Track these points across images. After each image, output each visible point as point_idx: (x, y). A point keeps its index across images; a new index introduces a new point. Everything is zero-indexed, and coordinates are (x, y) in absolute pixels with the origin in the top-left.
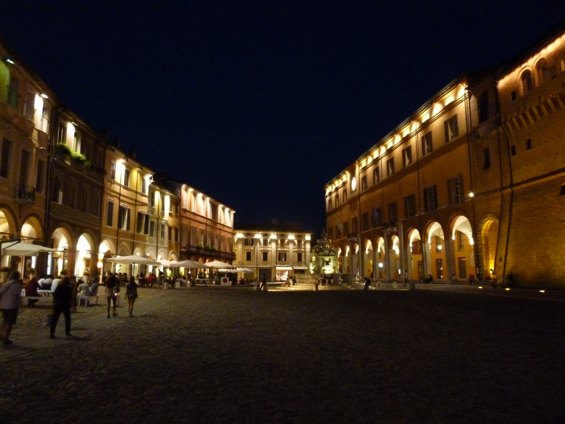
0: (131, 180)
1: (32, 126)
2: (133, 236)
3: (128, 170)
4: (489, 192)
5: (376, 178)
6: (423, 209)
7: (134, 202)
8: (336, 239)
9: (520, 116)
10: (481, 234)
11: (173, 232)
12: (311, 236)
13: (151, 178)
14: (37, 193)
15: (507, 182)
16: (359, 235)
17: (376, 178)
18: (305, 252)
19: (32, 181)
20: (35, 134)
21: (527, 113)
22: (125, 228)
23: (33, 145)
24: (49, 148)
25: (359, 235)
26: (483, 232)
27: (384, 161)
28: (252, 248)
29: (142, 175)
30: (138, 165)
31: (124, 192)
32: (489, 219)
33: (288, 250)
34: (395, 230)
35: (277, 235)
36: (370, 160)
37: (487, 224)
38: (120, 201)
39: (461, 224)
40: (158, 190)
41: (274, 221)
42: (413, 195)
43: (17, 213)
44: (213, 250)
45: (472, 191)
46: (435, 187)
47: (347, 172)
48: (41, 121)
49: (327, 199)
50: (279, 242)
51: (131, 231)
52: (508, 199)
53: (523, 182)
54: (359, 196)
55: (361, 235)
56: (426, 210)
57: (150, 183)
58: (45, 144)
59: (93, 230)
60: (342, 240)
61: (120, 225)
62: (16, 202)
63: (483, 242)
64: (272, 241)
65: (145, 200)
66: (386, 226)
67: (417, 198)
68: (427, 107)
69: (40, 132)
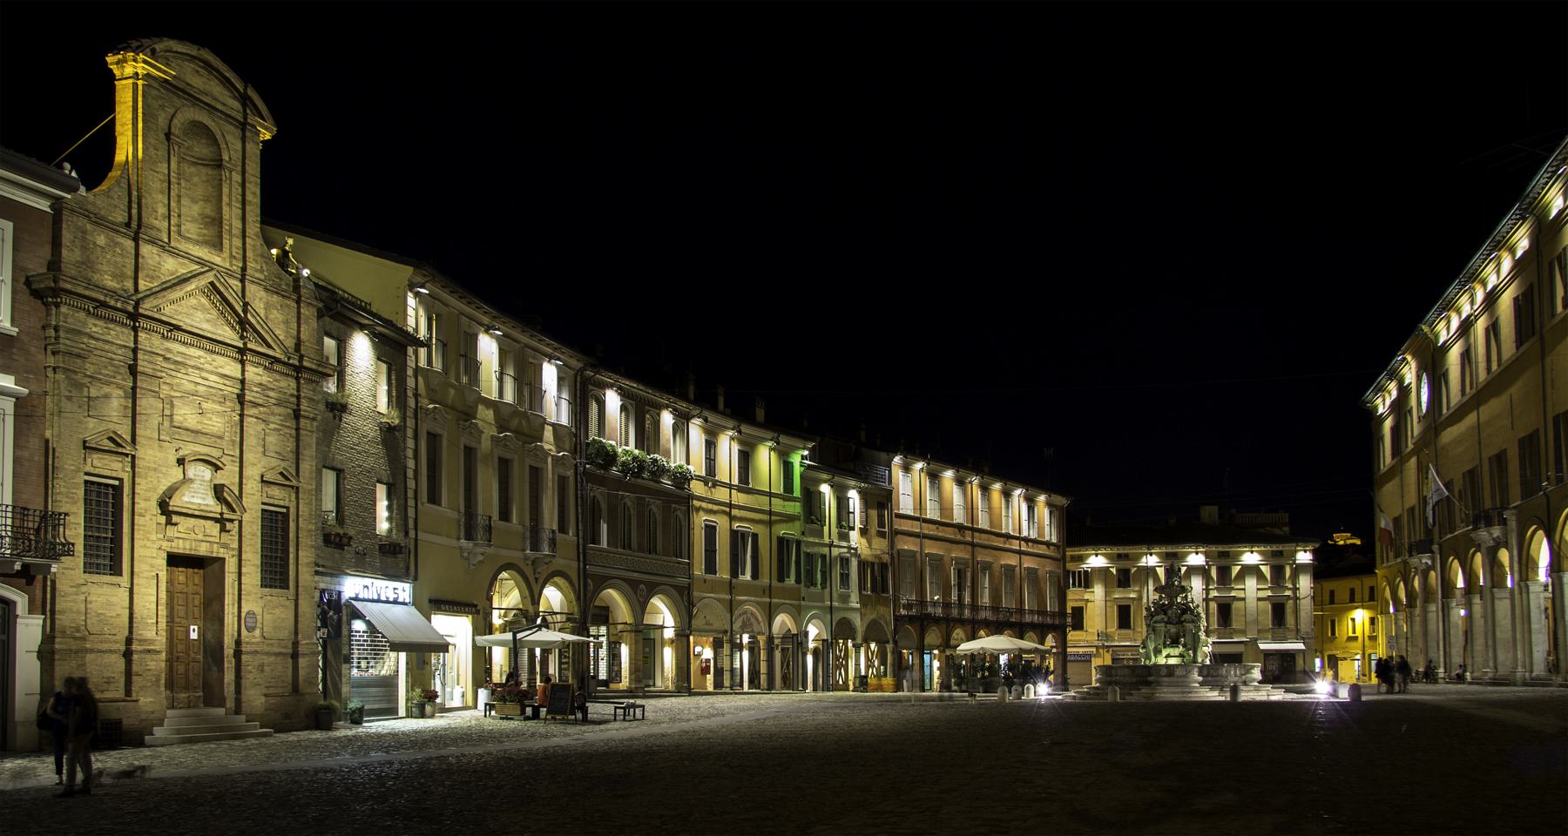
0: (755, 470)
1: (544, 422)
2: (769, 591)
7: (766, 517)
12: (1314, 552)
13: (803, 457)
14: (559, 536)
16: (1435, 547)
18: (1296, 598)
19: (550, 519)
20: (548, 433)
22: (748, 577)
23: (546, 454)
24: (574, 452)
25: (1435, 547)
28: (1133, 595)
30: (770, 435)
31: (739, 498)
33: (1241, 594)
35: (1207, 555)
41: (1210, 513)
43: (529, 572)
48: (556, 406)
55: (1440, 546)
58: (567, 446)
59: (675, 587)
61: (736, 569)
62: (526, 558)
64: (1193, 570)
69: (556, 427)
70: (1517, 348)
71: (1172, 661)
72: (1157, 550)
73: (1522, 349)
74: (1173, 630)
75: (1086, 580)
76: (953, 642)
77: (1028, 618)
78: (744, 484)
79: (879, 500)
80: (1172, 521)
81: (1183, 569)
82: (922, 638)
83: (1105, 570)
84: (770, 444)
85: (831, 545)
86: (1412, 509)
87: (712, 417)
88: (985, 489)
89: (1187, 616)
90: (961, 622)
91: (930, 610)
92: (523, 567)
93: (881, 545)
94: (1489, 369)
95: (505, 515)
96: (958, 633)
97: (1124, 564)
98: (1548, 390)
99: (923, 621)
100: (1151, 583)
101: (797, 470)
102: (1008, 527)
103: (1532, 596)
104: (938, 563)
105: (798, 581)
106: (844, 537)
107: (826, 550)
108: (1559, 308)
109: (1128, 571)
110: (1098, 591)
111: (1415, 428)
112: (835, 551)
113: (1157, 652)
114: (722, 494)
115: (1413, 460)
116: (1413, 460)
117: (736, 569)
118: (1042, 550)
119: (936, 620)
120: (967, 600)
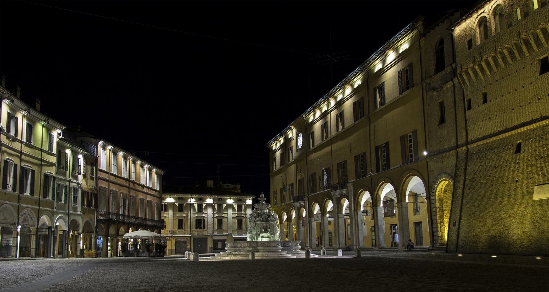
0: (35, 135)
3: (31, 123)
4: (445, 151)
5: (325, 134)
6: (374, 168)
7: (39, 162)
8: (282, 202)
9: (476, 67)
10: (435, 196)
12: (253, 200)
15: (462, 140)
16: (306, 199)
17: (325, 134)
18: (246, 218)
21: (483, 64)
25: (306, 199)
26: (437, 194)
27: (333, 114)
28: (184, 215)
29: (49, 130)
30: (44, 118)
31: (26, 150)
32: (444, 180)
33: (226, 216)
34: (344, 191)
35: (213, 199)
36: (318, 114)
37: (443, 184)
39: (415, 184)
40: (68, 148)
41: (210, 183)
42: (365, 153)
44: (137, 218)
45: (426, 150)
46: (387, 144)
47: (293, 127)
50: (216, 207)
51: (36, 196)
52: (462, 156)
53: (479, 140)
56: (378, 170)
57: (58, 139)
60: (287, 205)
63: (438, 205)
64: (208, 205)
65: (53, 159)
66: (335, 188)
67: (368, 156)
68: (380, 55)
70: (355, 121)
71: (265, 239)
72: (195, 196)
73: (357, 122)
74: (265, 225)
75: (165, 208)
76: (120, 233)
77: (149, 223)
78: (29, 143)
79: (92, 161)
80: (197, 186)
81: (204, 205)
83: (173, 204)
84: (43, 123)
85: (70, 181)
86: (292, 185)
87: (16, 101)
88: (134, 163)
89: (271, 218)
90: (124, 223)
91: (111, 217)
93: (92, 183)
94: (337, 130)
96: (122, 229)
97: (181, 202)
98: (372, 137)
99: (108, 222)
100: (192, 210)
101: (55, 140)
102: (142, 182)
103: (359, 216)
104: (115, 193)
105: (53, 198)
106: (76, 178)
107: (67, 183)
108: (378, 107)
109: (183, 205)
110: (170, 212)
111: (294, 154)
112: (72, 185)
113: (258, 235)
115: (293, 166)
116: (293, 166)
118: (153, 193)
120: (126, 213)
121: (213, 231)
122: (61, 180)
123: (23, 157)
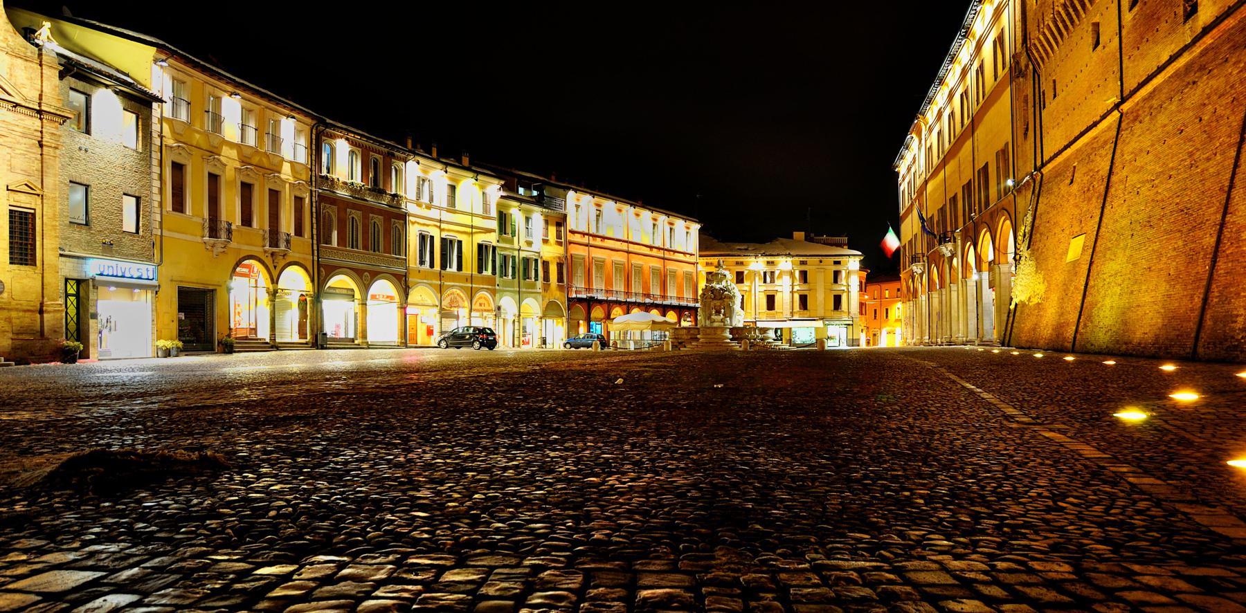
2: (471, 279)
7: (469, 230)
11: (553, 270)
14: (294, 238)
19: (287, 224)
20: (286, 168)
23: (284, 182)
38: (442, 230)
43: (269, 261)
49: (901, 188)
50: (797, 274)
53: (1052, 159)
54: (926, 182)
82: (589, 313)
92: (263, 258)
93: (560, 251)
95: (247, 220)
105: (494, 272)
107: (516, 253)
112: (523, 254)
114: (434, 213)
117: (443, 267)
119: (600, 302)
121: (792, 313)
122: (505, 249)
123: (443, 226)
